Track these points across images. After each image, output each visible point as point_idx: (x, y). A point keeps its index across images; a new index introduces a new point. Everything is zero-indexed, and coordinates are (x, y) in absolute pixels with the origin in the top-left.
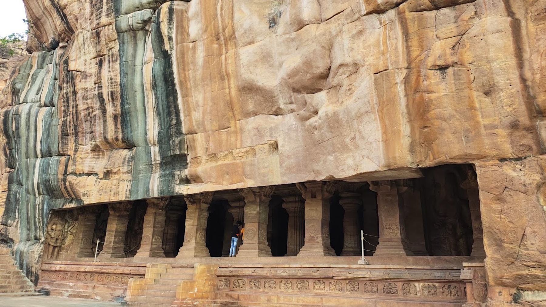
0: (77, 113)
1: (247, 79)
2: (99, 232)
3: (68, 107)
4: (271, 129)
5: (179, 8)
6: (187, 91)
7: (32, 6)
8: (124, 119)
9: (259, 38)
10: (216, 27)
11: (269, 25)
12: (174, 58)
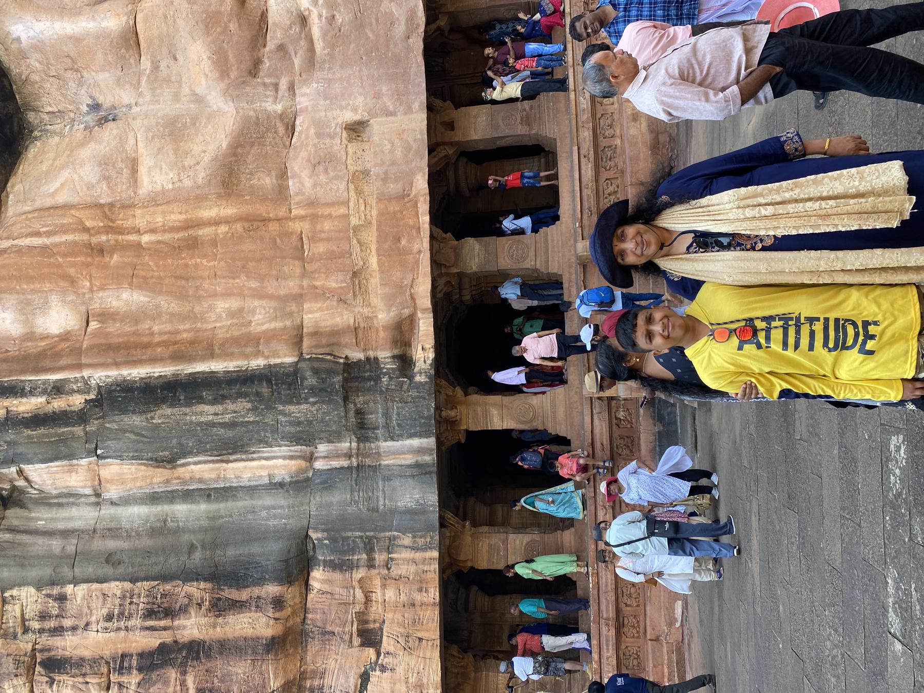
4: (319, 135)
6: (200, 343)
9: (131, 141)
10: (72, 249)
11: (111, 125)
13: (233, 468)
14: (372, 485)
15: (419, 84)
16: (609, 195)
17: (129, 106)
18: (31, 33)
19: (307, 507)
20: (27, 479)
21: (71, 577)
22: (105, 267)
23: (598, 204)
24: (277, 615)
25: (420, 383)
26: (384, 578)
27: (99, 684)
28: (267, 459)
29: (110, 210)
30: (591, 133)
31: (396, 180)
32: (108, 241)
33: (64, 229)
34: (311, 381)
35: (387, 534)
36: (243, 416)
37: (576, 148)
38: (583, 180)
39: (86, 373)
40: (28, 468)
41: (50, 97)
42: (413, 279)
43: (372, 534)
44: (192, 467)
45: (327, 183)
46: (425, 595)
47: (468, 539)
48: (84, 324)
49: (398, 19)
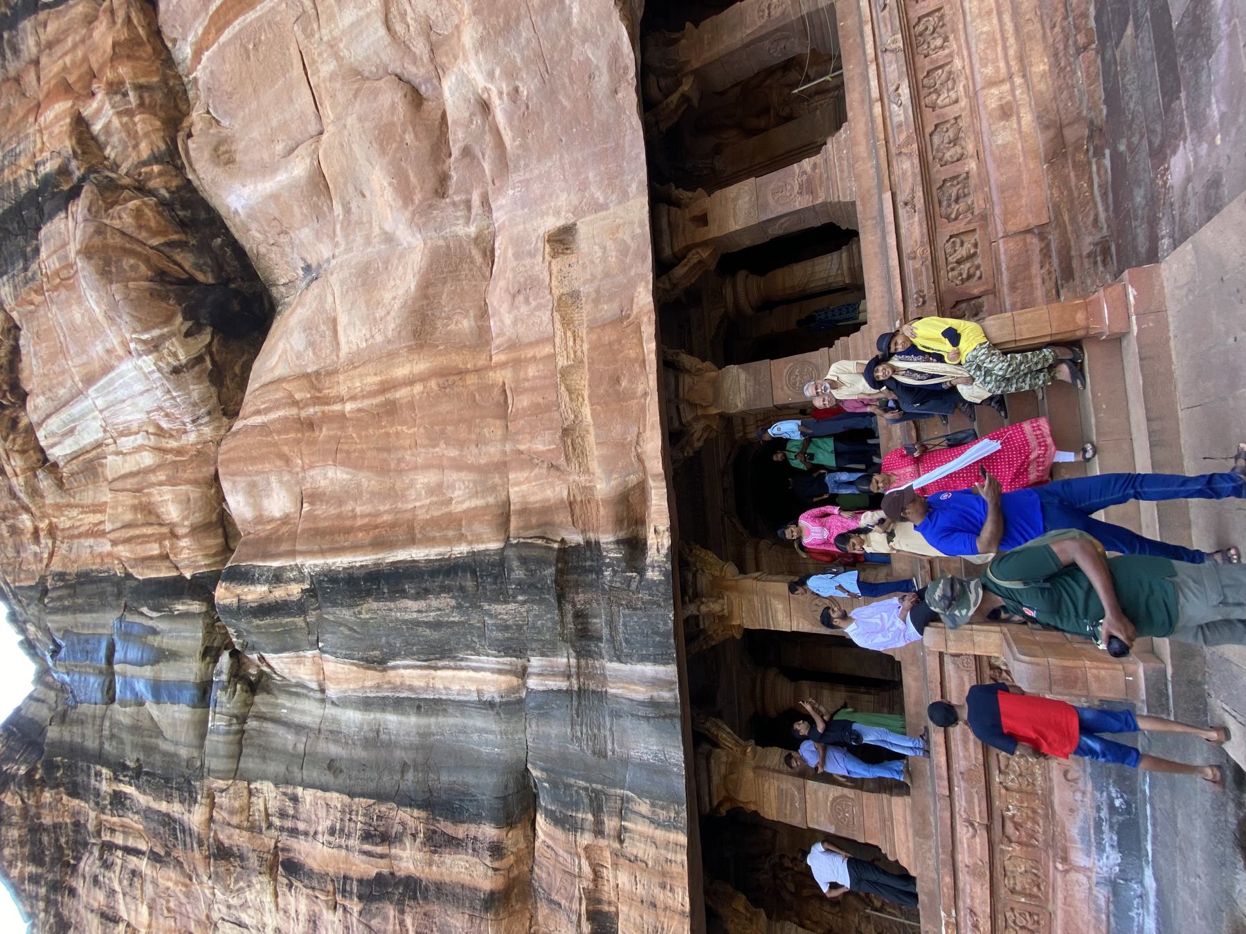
1: (398, 322)
4: (517, 256)
9: (330, 299)
13: (442, 678)
14: (598, 719)
15: (638, 155)
16: (959, 262)
17: (328, 261)
18: (243, 202)
19: (522, 736)
20: (269, 666)
21: (299, 779)
22: (313, 442)
23: (936, 282)
24: (496, 865)
25: (654, 581)
26: (615, 854)
27: (327, 902)
28: (475, 669)
29: (317, 379)
30: (916, 161)
31: (610, 299)
32: (316, 413)
33: (277, 406)
34: (519, 573)
35: (619, 791)
36: (448, 615)
37: (889, 194)
38: (907, 247)
39: (299, 561)
40: (266, 655)
41: (280, 267)
42: (639, 433)
43: (599, 787)
44: (402, 671)
45: (528, 316)
46: (670, 894)
47: (749, 774)
49: (597, 67)
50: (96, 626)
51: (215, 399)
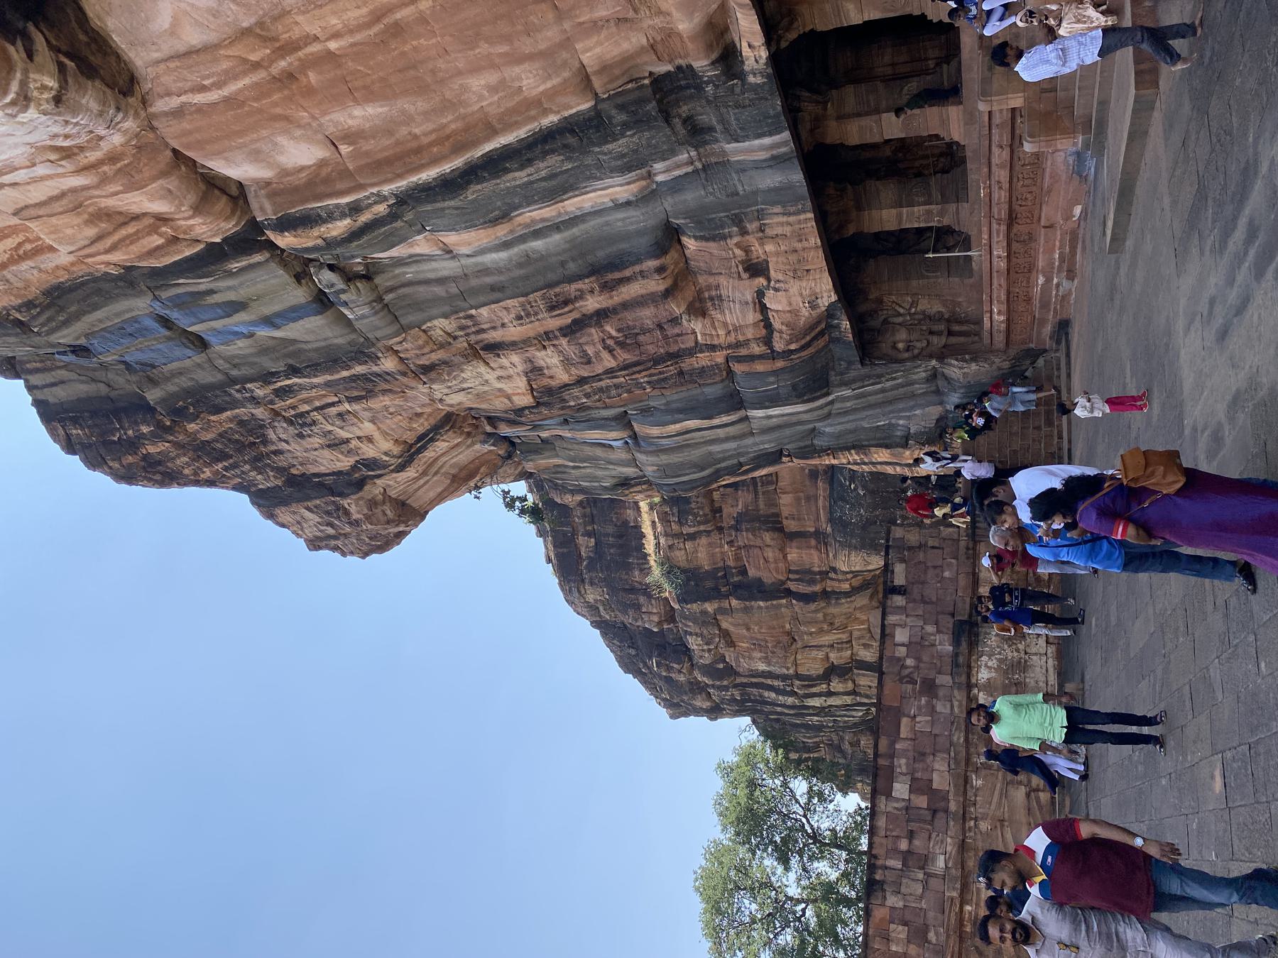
0: (625, 367)
2: (904, 244)
3: (617, 386)
5: (268, 207)
7: (432, 494)
8: (606, 268)
10: (260, 91)
12: (402, 184)
22: (309, 92)
29: (262, 29)
34: (621, 117)
48: (333, 148)
50: (117, 315)
51: (108, 91)
